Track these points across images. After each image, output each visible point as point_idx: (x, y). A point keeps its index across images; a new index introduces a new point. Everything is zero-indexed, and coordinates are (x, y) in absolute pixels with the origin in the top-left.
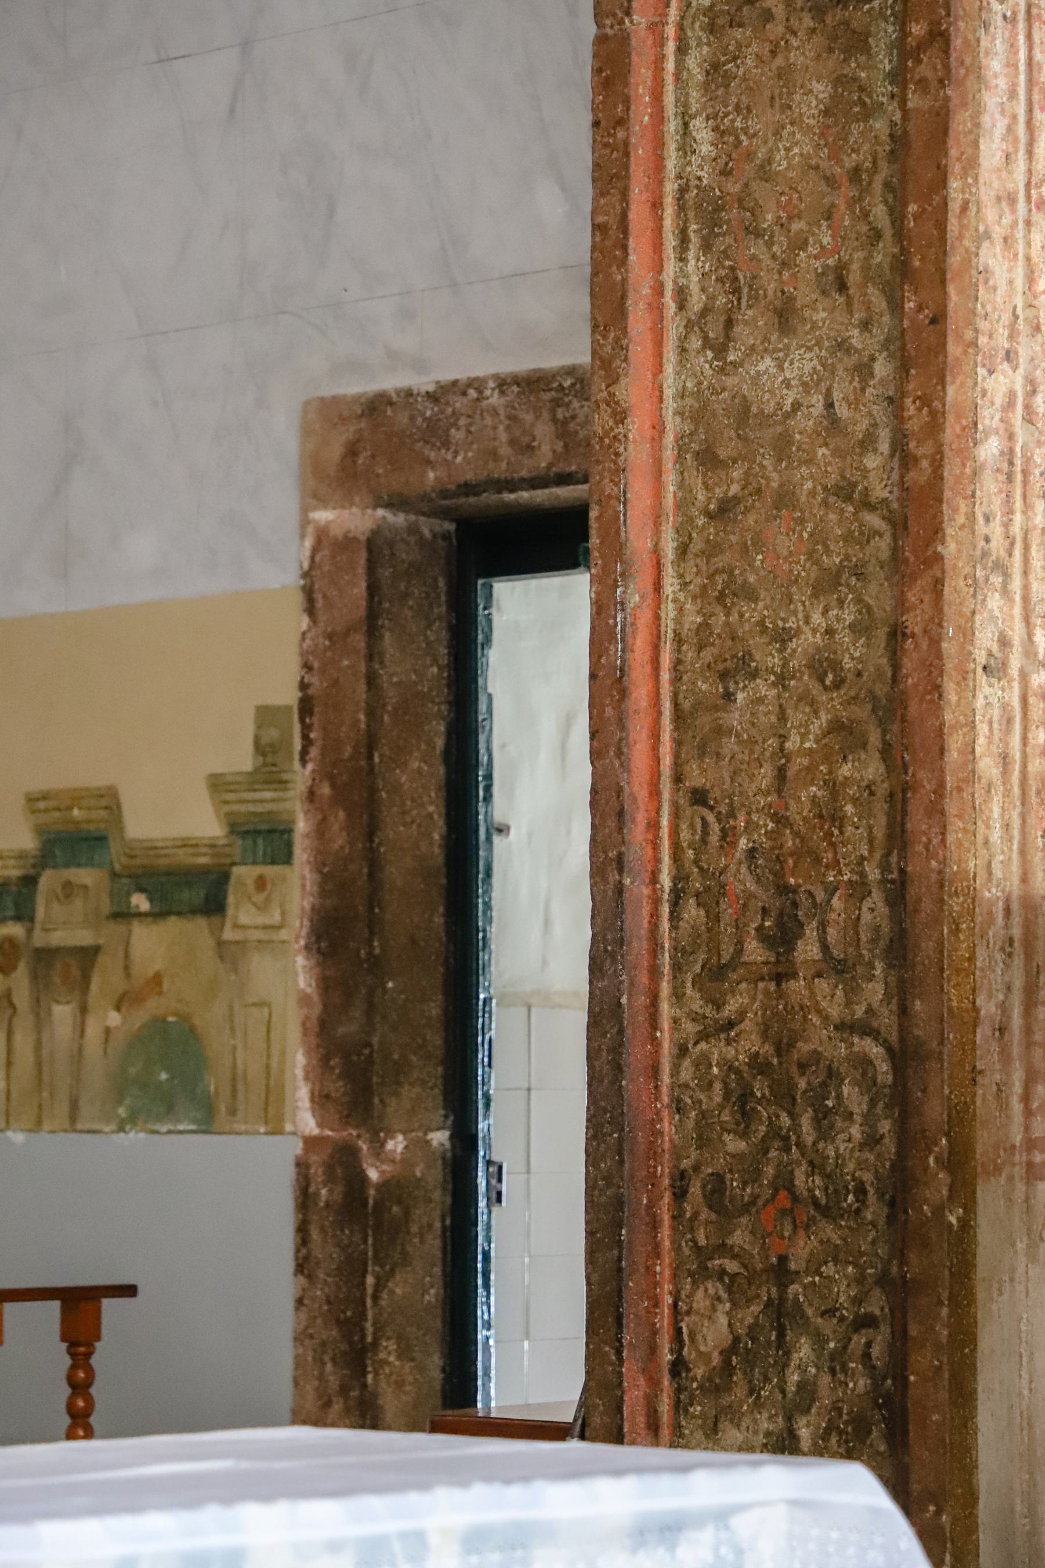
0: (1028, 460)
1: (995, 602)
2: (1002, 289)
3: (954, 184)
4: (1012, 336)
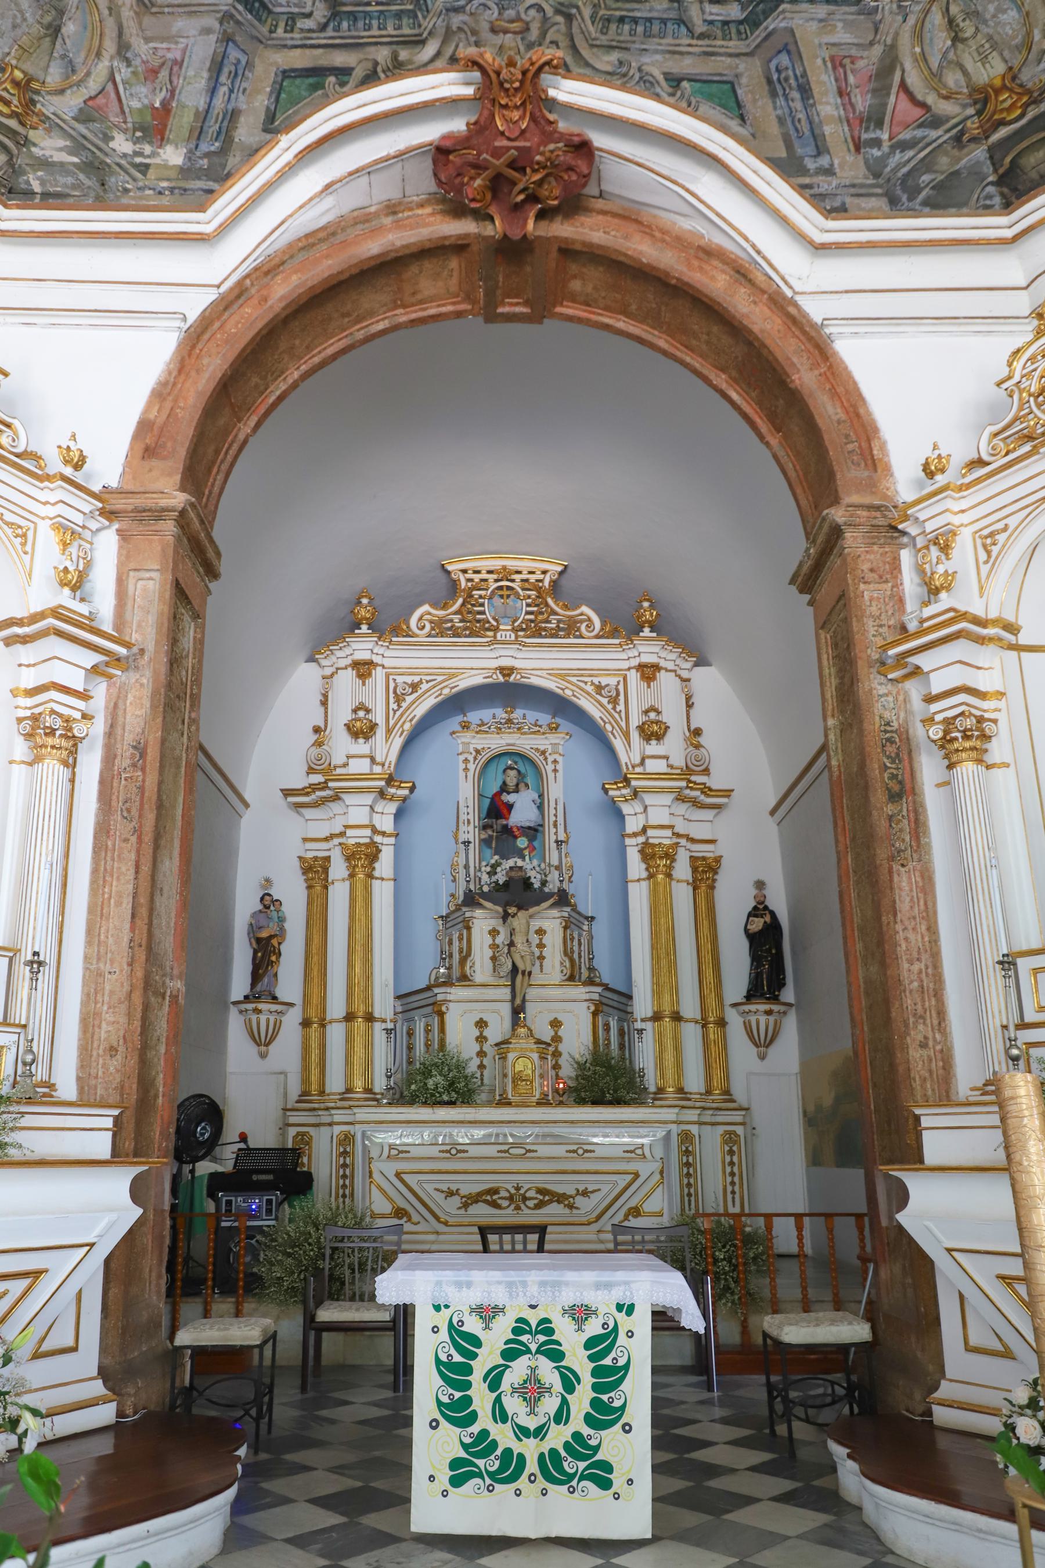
0: (928, 987)
1: (921, 1027)
2: (913, 942)
3: (884, 918)
4: (919, 953)
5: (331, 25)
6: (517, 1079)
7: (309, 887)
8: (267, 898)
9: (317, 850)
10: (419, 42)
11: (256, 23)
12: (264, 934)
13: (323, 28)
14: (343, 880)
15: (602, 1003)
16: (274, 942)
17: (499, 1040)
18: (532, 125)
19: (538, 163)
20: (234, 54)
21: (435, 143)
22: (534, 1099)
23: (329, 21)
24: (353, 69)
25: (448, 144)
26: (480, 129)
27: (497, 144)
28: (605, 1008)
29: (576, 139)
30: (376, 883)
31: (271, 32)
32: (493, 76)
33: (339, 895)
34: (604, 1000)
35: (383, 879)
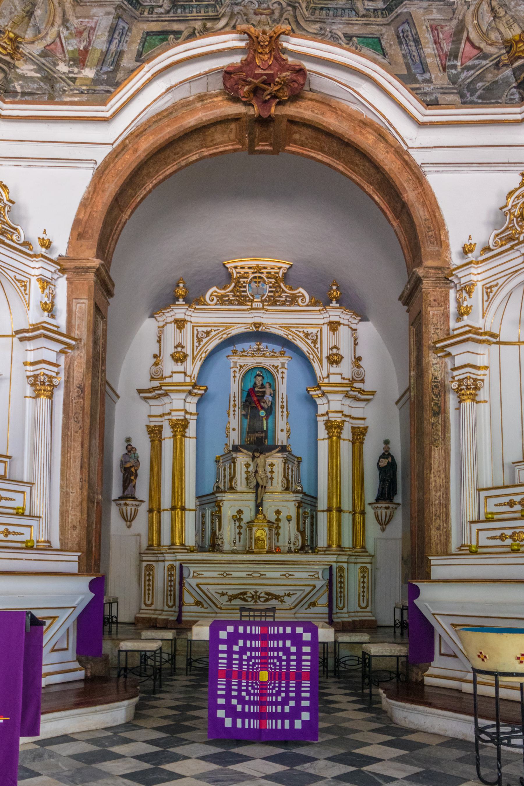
5: (172, 11)
6: (258, 539)
7: (152, 441)
8: (129, 447)
9: (155, 422)
10: (217, 19)
11: (134, 10)
12: (128, 465)
13: (168, 12)
14: (170, 438)
15: (302, 502)
16: (133, 470)
17: (249, 520)
18: (275, 61)
19: (277, 82)
20: (121, 24)
21: (225, 69)
22: (265, 550)
23: (171, 9)
24: (183, 31)
25: (231, 69)
26: (248, 63)
27: (256, 72)
28: (304, 505)
29: (297, 67)
30: (187, 440)
31: (141, 14)
32: (255, 39)
33: (167, 446)
34: (303, 500)
35: (190, 438)
